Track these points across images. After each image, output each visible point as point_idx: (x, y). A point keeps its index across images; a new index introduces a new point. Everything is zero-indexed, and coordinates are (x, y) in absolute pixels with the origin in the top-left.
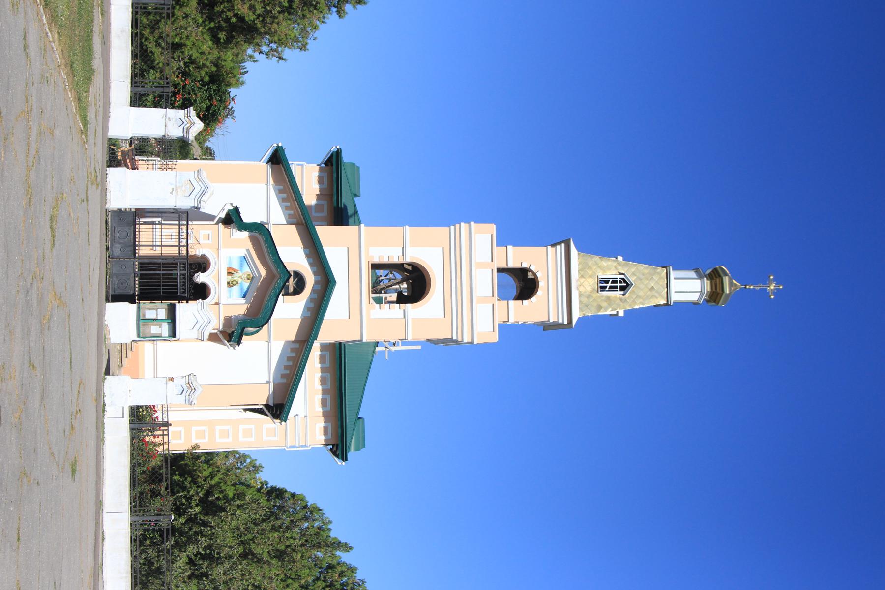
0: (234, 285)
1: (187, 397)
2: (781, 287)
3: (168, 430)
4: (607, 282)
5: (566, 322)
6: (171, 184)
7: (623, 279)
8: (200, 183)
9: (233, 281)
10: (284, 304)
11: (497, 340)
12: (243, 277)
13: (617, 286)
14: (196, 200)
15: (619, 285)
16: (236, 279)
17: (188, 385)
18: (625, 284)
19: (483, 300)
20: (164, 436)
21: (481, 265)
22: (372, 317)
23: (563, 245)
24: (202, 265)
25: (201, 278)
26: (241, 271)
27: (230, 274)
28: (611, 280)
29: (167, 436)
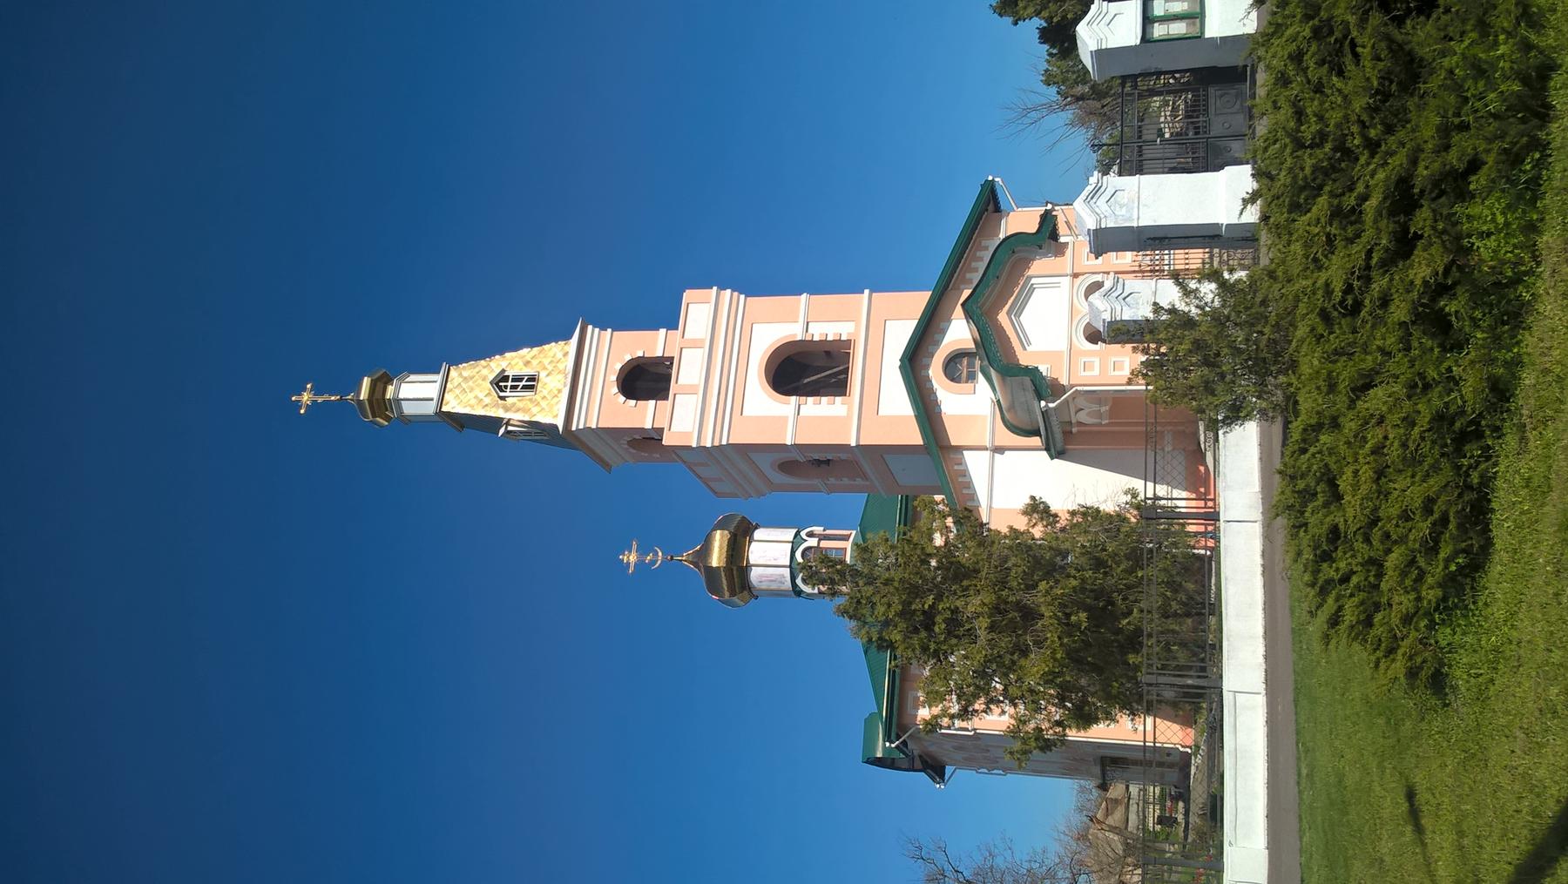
2: (293, 399)
4: (524, 387)
5: (590, 327)
11: (685, 294)
13: (512, 381)
15: (509, 384)
18: (501, 384)
21: (691, 390)
23: (574, 428)
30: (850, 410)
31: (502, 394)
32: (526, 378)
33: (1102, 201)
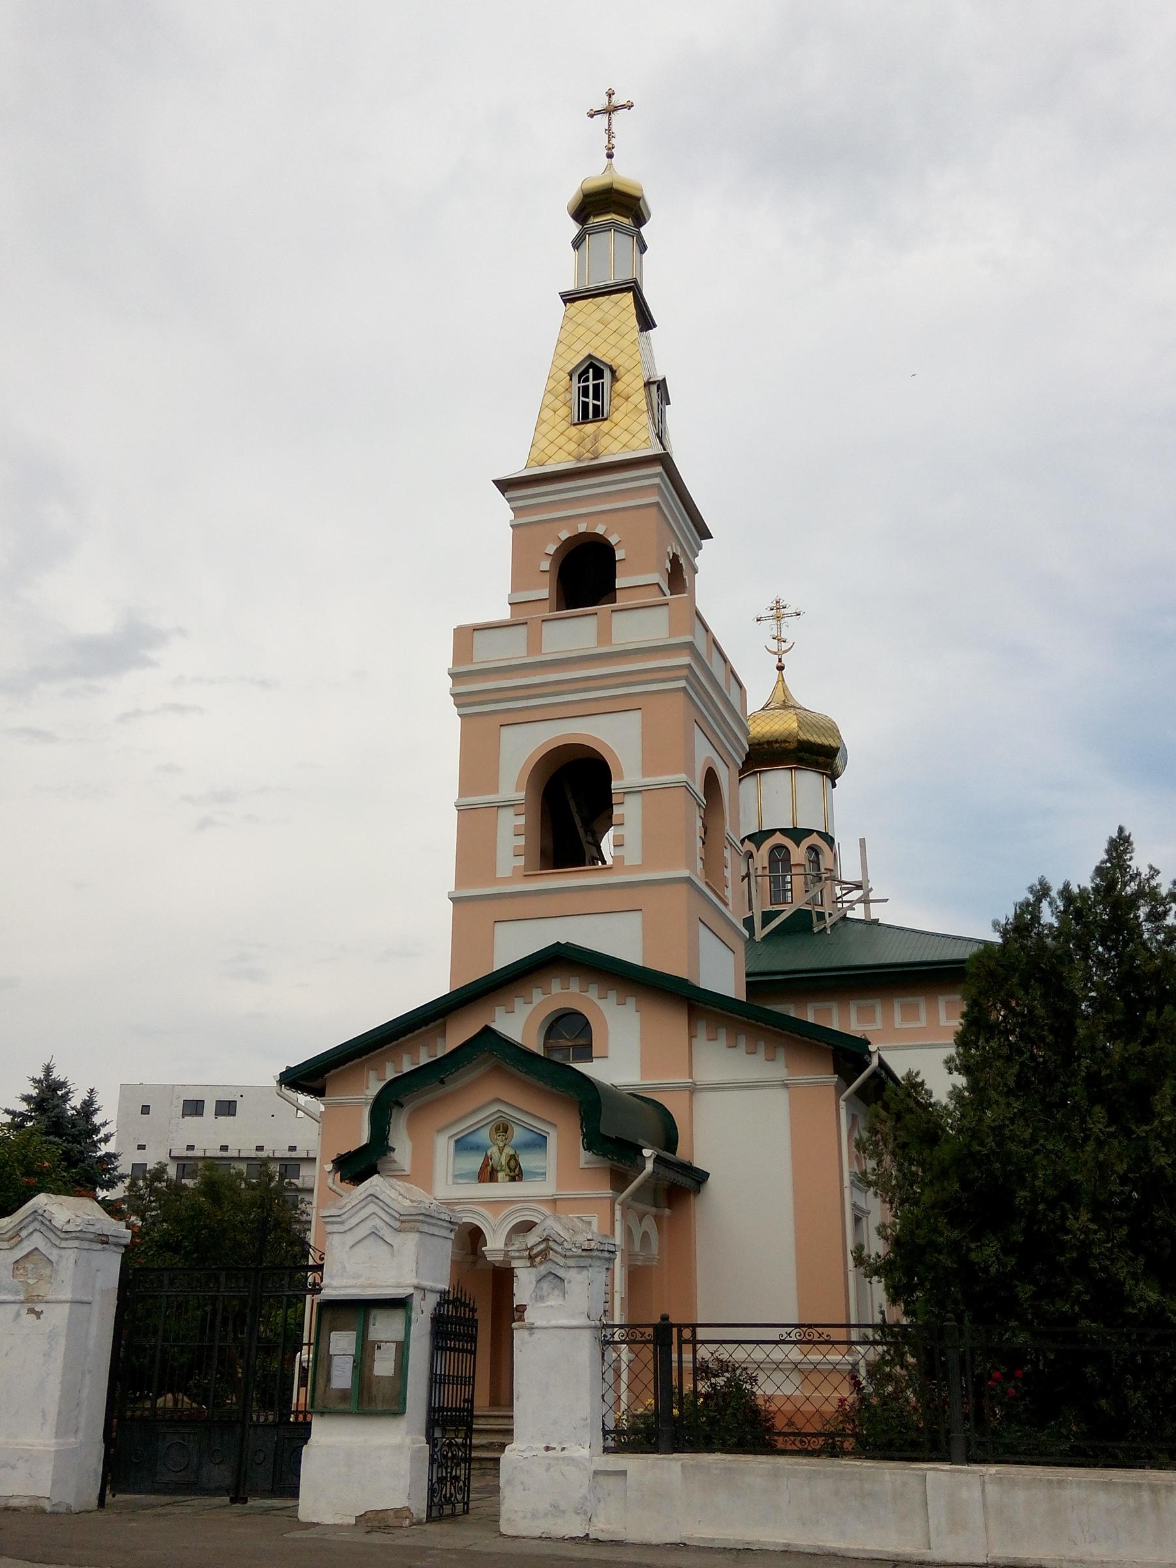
0: (518, 1164)
1: (570, 1262)
3: (680, 1327)
6: (18, 1315)
8: (24, 1234)
9: (509, 1168)
10: (609, 1056)
12: (501, 1144)
13: (594, 385)
14: (64, 1244)
16: (504, 1161)
17: (538, 1260)
18: (591, 370)
19: (604, 633)
20: (700, 1337)
22: (639, 862)
26: (489, 1147)
28: (582, 398)
29: (698, 1329)
30: (505, 880)
32: (599, 403)
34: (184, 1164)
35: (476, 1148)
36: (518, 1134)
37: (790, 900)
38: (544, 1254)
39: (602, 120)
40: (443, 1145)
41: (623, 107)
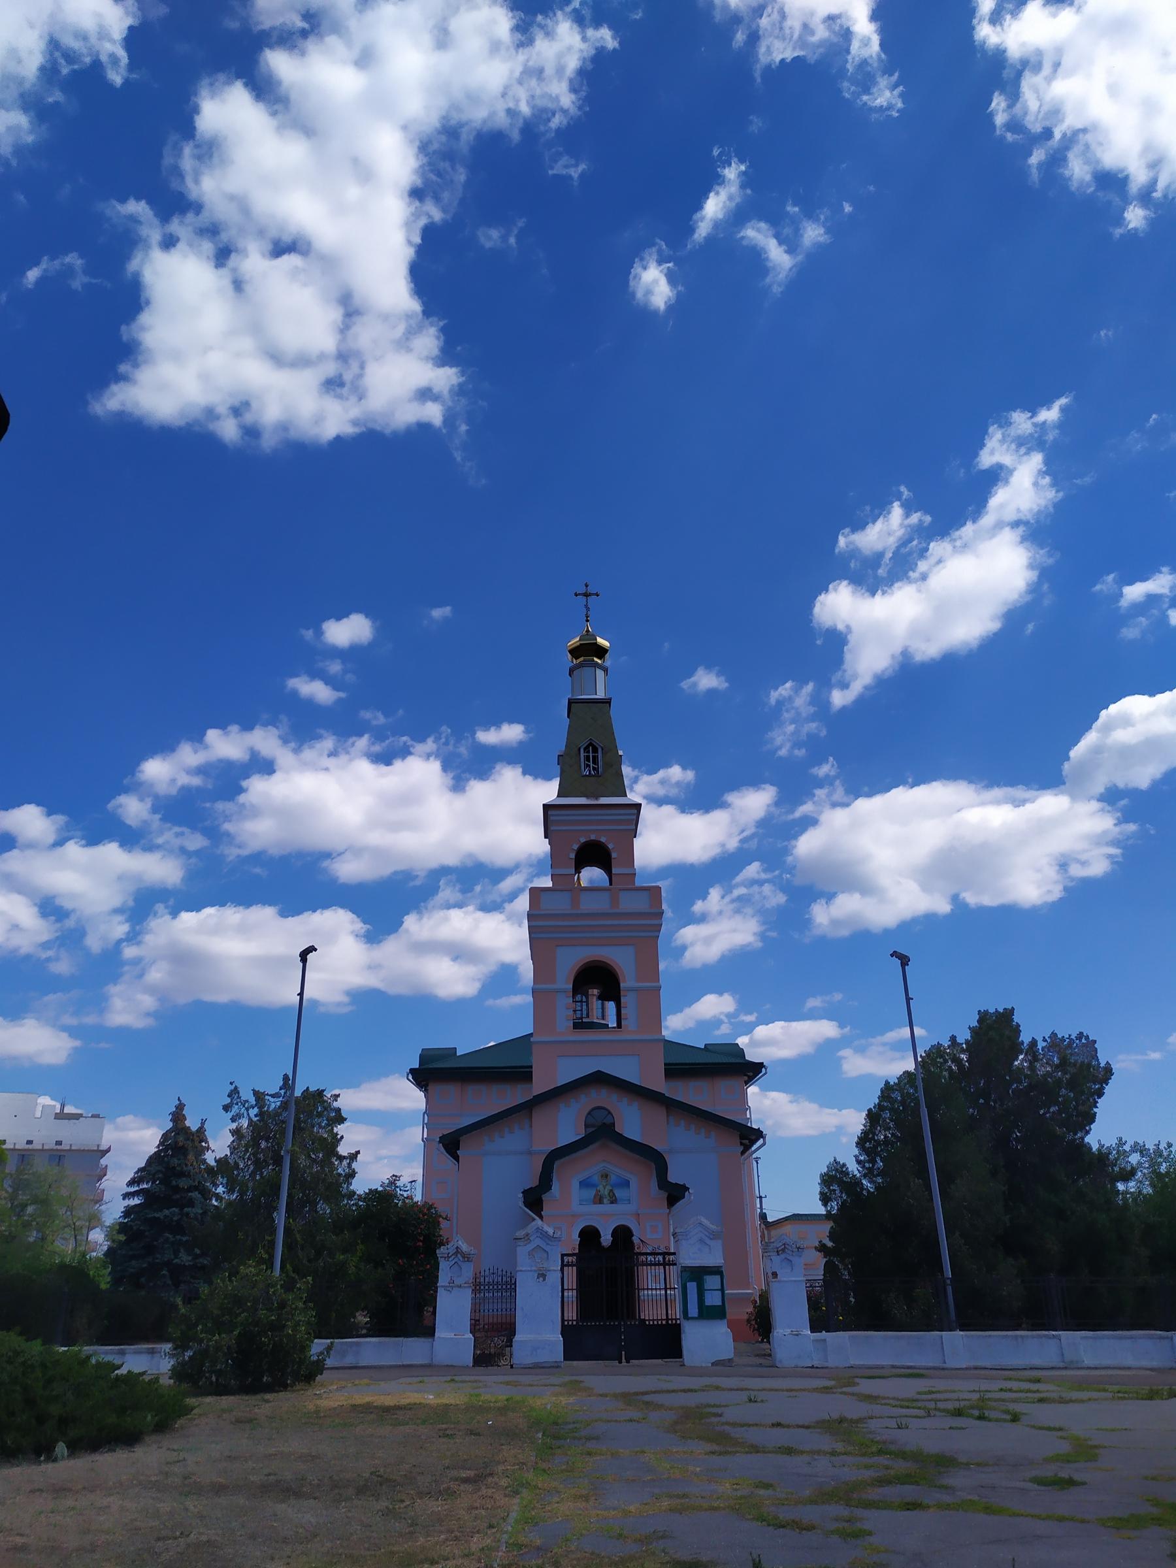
0: (614, 1194)
7: (585, 749)
16: (606, 1193)
24: (589, 1236)
25: (606, 1239)
27: (601, 1202)
31: (582, 750)
33: (538, 1242)
34: (23, 1155)
35: (594, 1186)
36: (613, 1178)
37: (613, 1023)
38: (783, 1250)
39: (582, 599)
40: (575, 1184)
41: (593, 594)
